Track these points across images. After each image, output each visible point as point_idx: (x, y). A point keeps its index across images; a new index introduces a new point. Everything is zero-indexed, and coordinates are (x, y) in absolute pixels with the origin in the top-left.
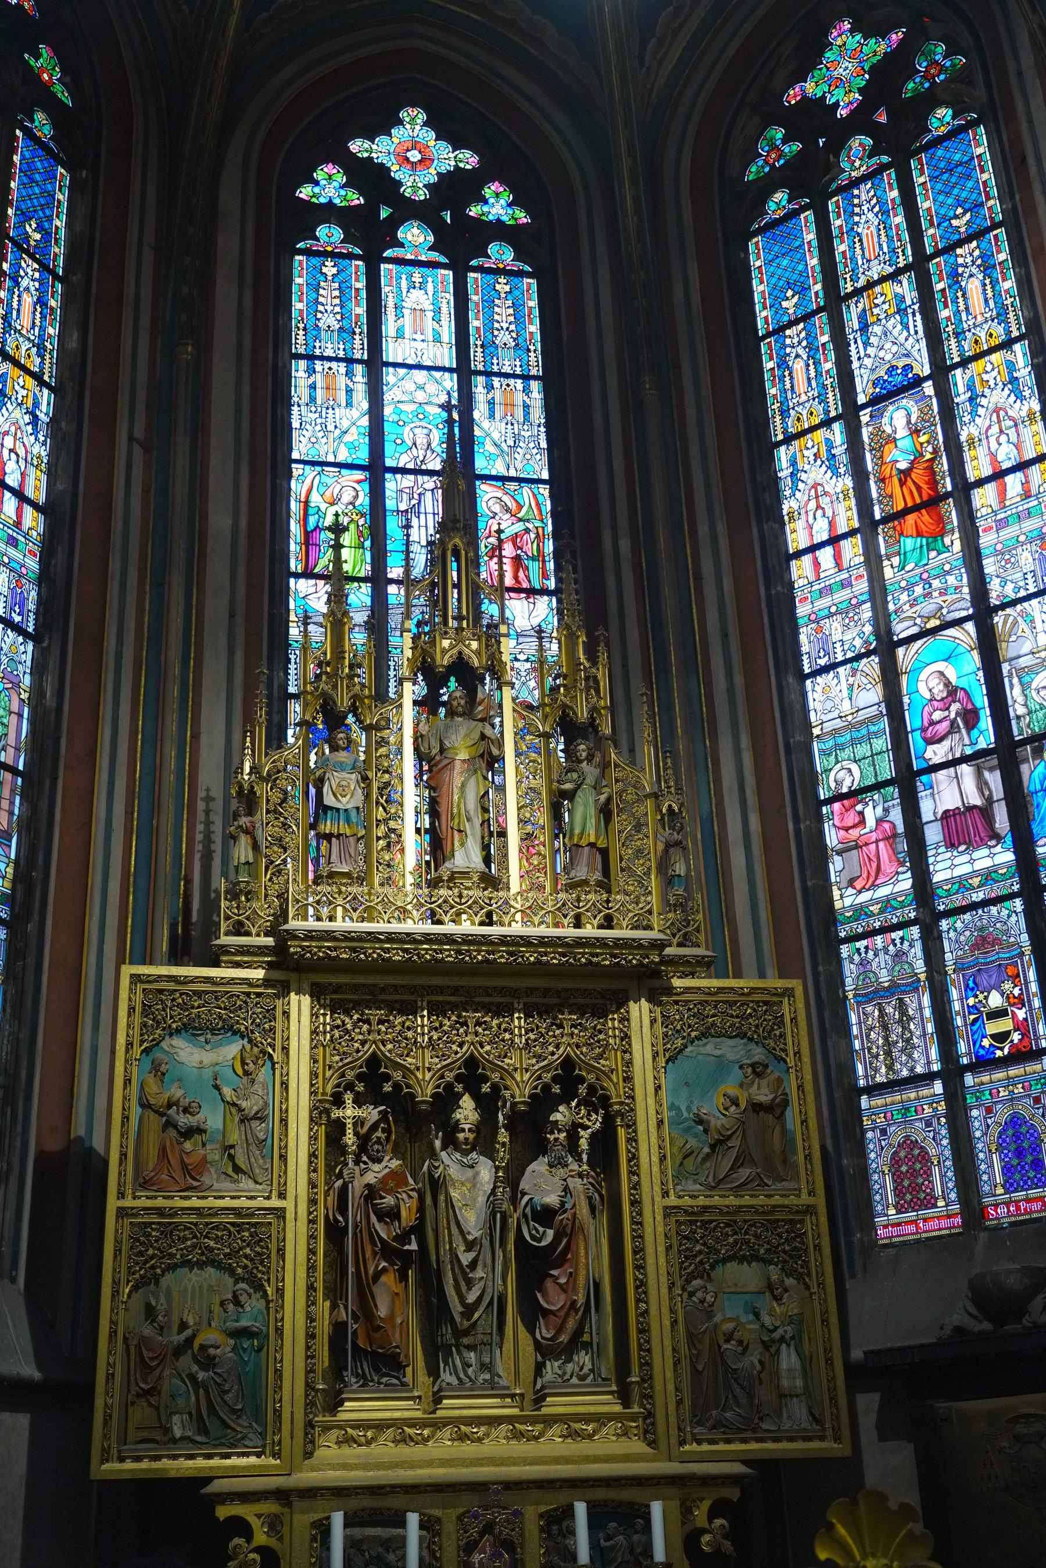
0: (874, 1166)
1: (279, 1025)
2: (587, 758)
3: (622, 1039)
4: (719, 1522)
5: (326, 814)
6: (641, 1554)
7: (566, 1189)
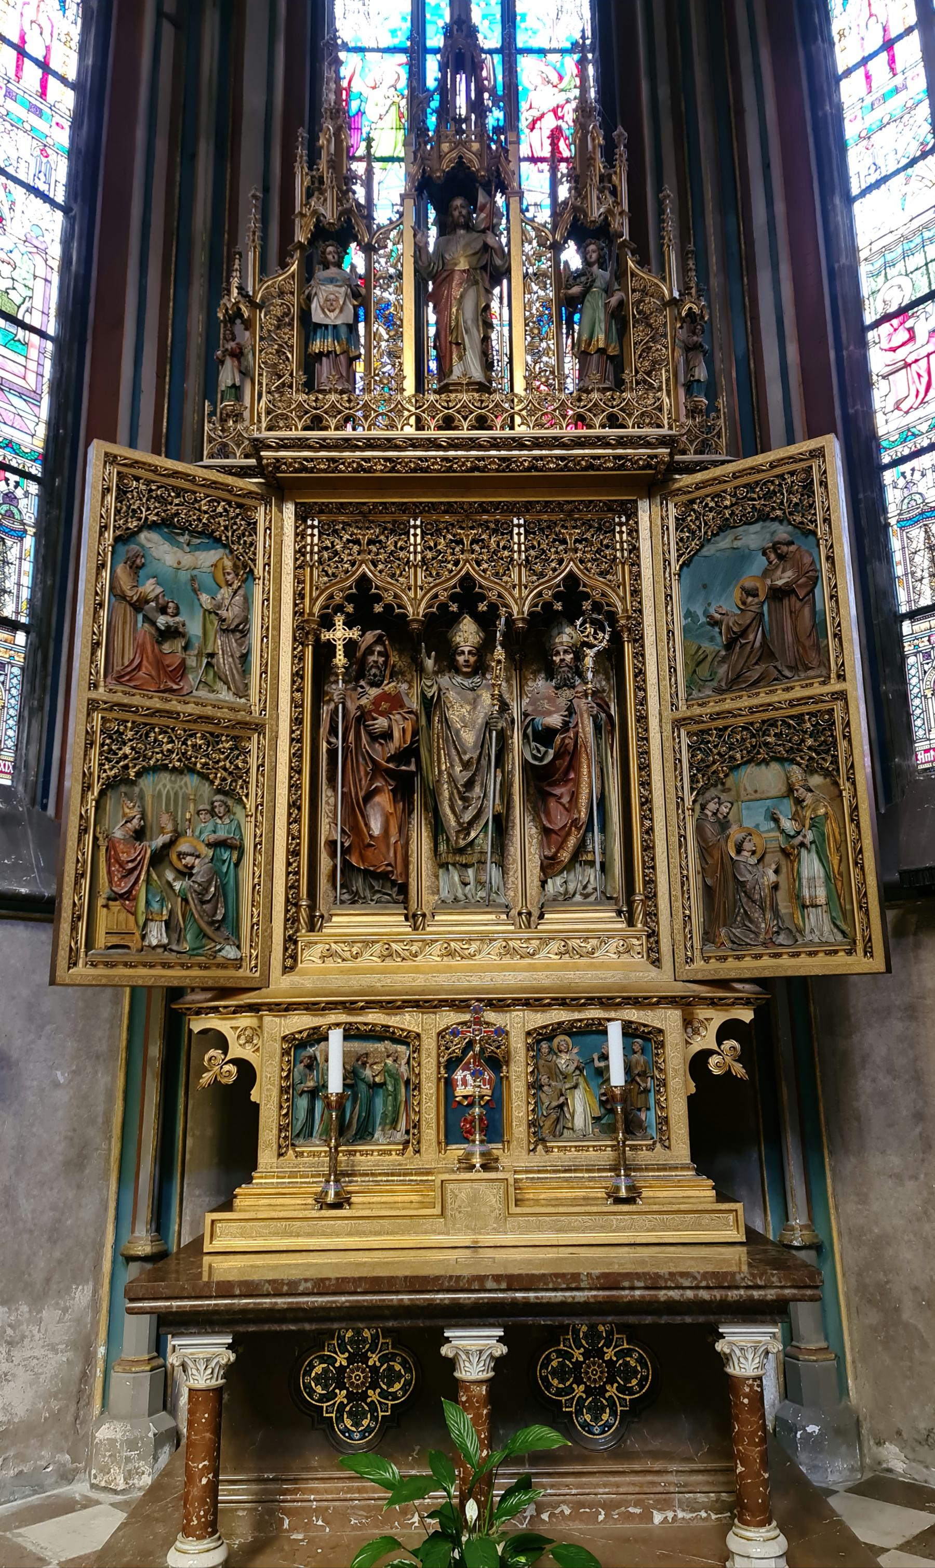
0: (916, 690)
2: (598, 261)
3: (630, 552)
4: (728, 1044)
5: (315, 333)
6: (639, 1075)
7: (571, 711)
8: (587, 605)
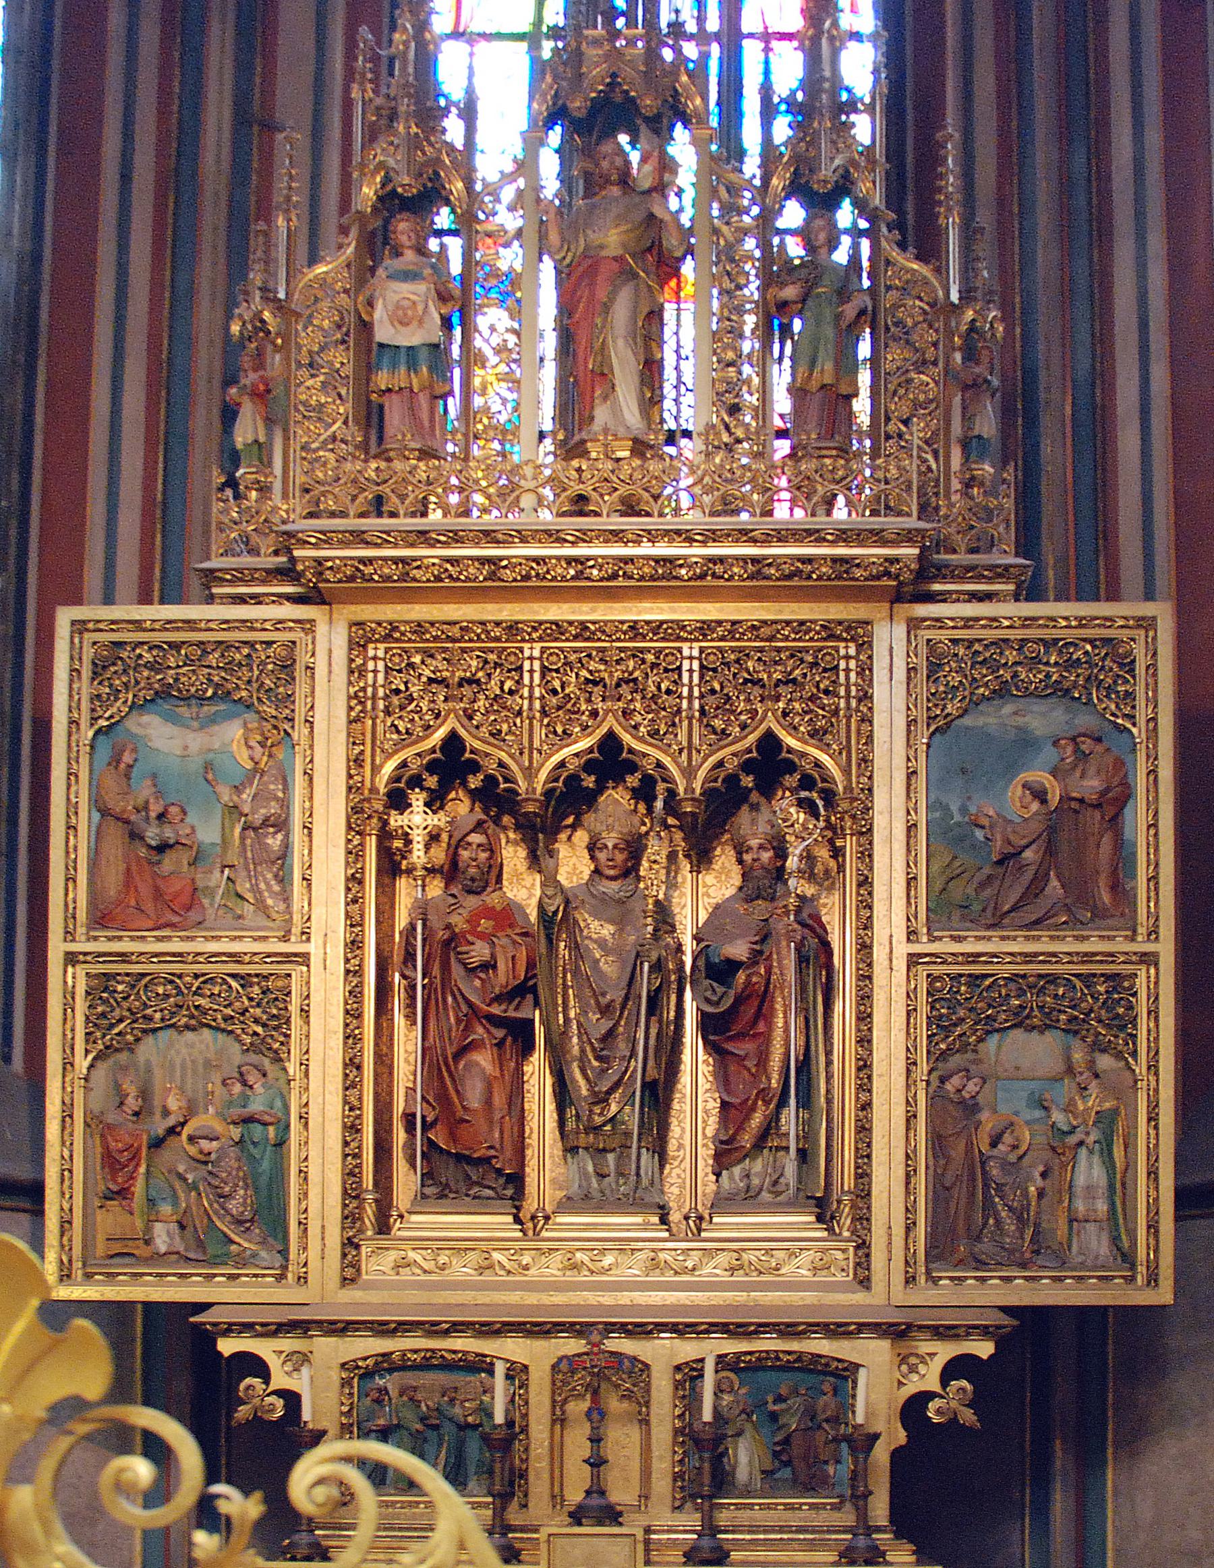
1: (301, 689)
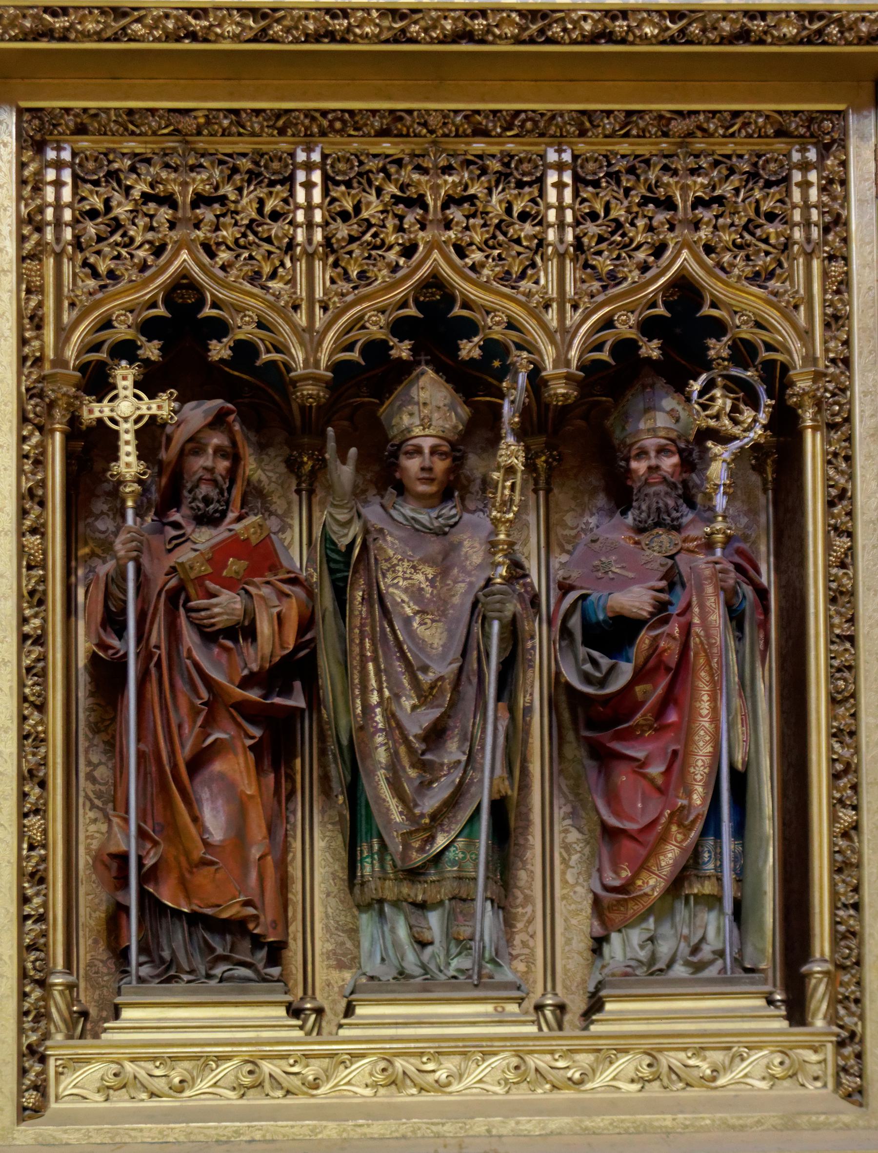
3: (827, 230)
8: (718, 348)
